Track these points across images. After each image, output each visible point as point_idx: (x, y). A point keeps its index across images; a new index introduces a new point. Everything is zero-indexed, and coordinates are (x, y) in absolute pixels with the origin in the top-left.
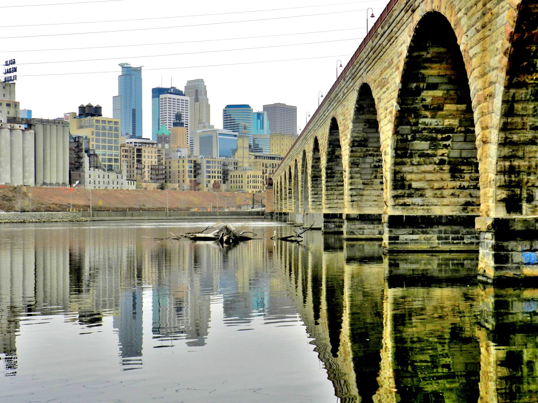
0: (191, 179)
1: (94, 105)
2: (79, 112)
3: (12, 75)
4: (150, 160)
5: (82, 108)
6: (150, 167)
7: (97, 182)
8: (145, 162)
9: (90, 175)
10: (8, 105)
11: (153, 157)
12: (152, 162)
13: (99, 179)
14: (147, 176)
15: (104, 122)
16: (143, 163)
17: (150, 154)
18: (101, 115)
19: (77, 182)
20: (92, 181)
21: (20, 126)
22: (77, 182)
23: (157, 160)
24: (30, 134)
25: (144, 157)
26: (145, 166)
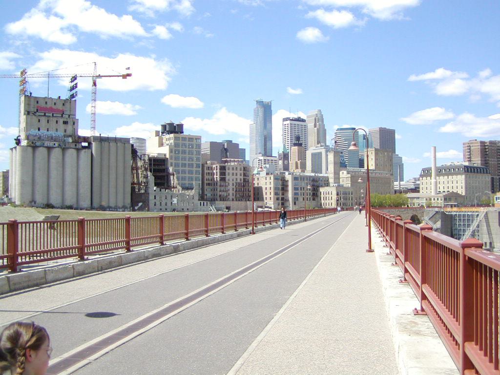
0: (278, 196)
1: (176, 123)
2: (162, 129)
3: (74, 91)
4: (235, 177)
5: (164, 127)
6: (235, 184)
7: (163, 203)
8: (229, 180)
9: (155, 196)
10: (65, 123)
11: (238, 174)
12: (237, 179)
13: (166, 201)
14: (231, 194)
15: (184, 139)
16: (227, 181)
17: (235, 172)
18: (183, 133)
19: (140, 204)
20: (158, 203)
21: (76, 145)
22: (140, 204)
23: (242, 177)
24: (85, 155)
25: (229, 175)
26: (228, 184)
